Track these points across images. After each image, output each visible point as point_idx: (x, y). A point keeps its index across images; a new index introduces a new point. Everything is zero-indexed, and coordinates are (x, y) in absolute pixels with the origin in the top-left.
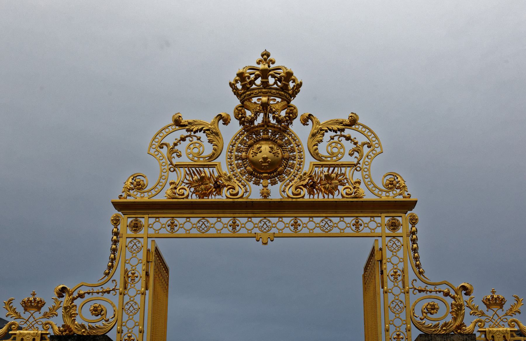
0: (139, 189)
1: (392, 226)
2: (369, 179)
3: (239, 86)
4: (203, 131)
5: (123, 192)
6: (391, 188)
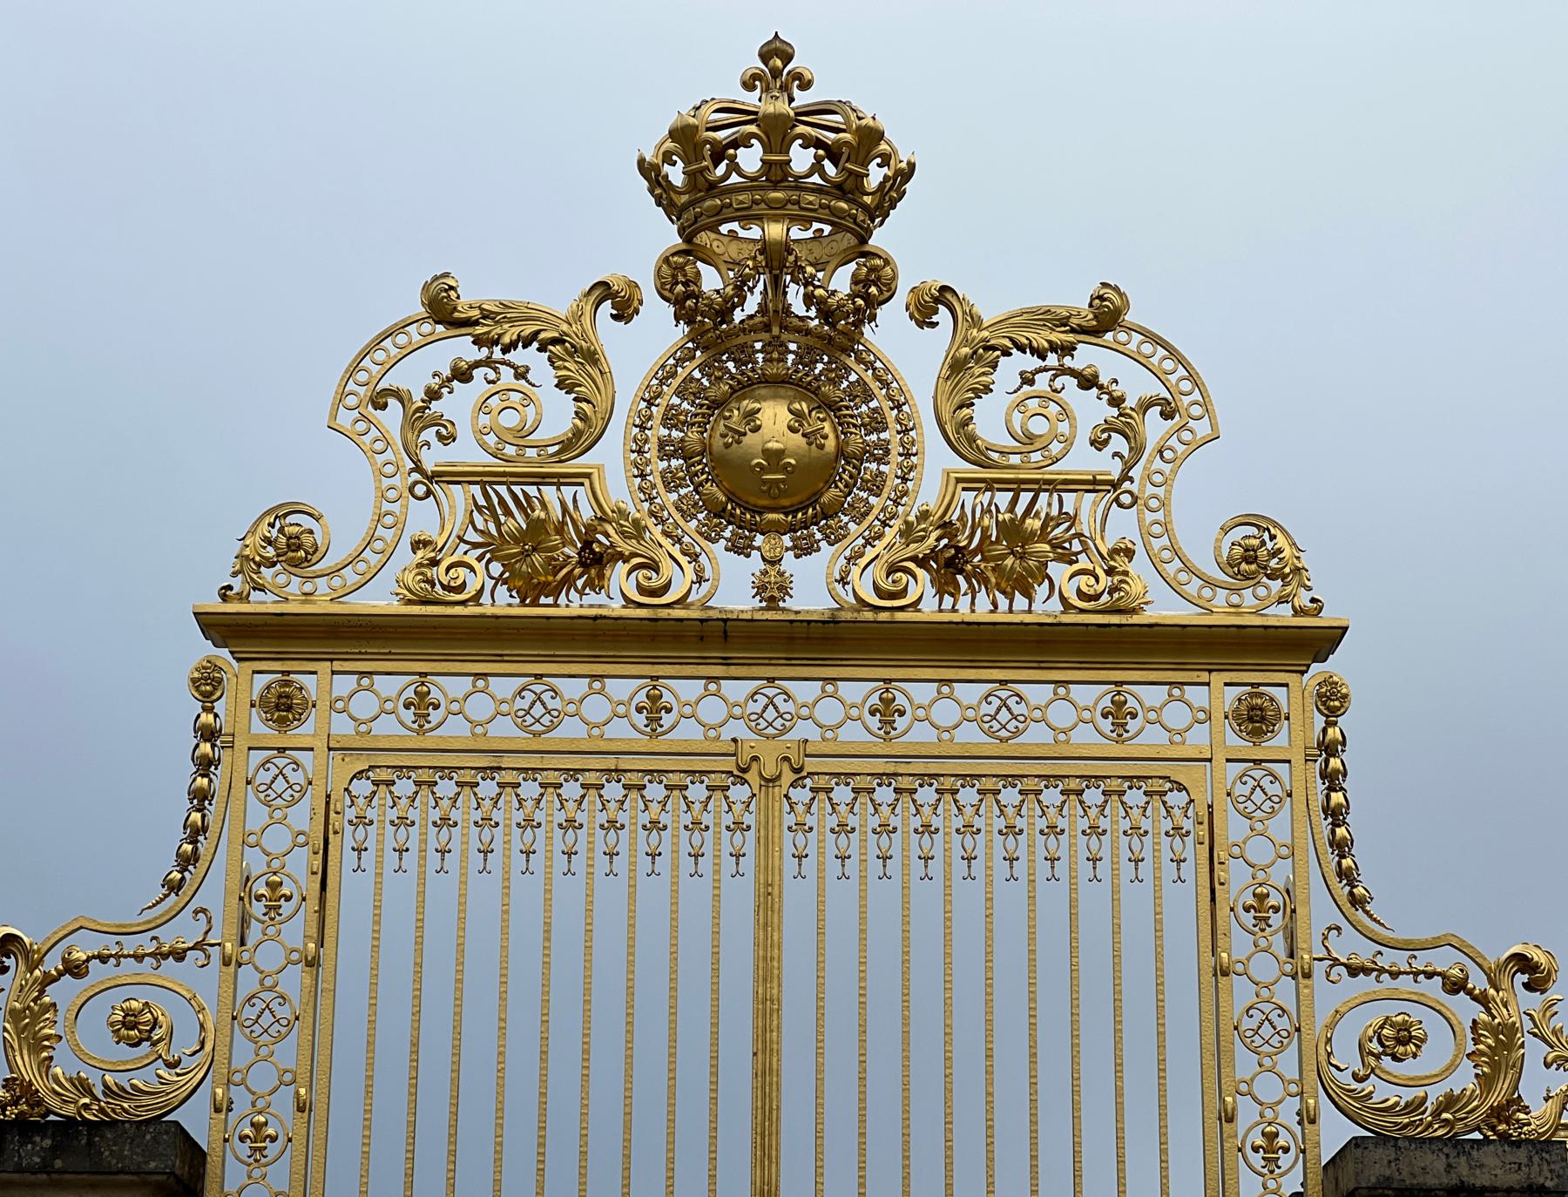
0: (296, 564)
1: (1251, 719)
2: (1165, 541)
3: (676, 174)
4: (535, 345)
5: (235, 574)
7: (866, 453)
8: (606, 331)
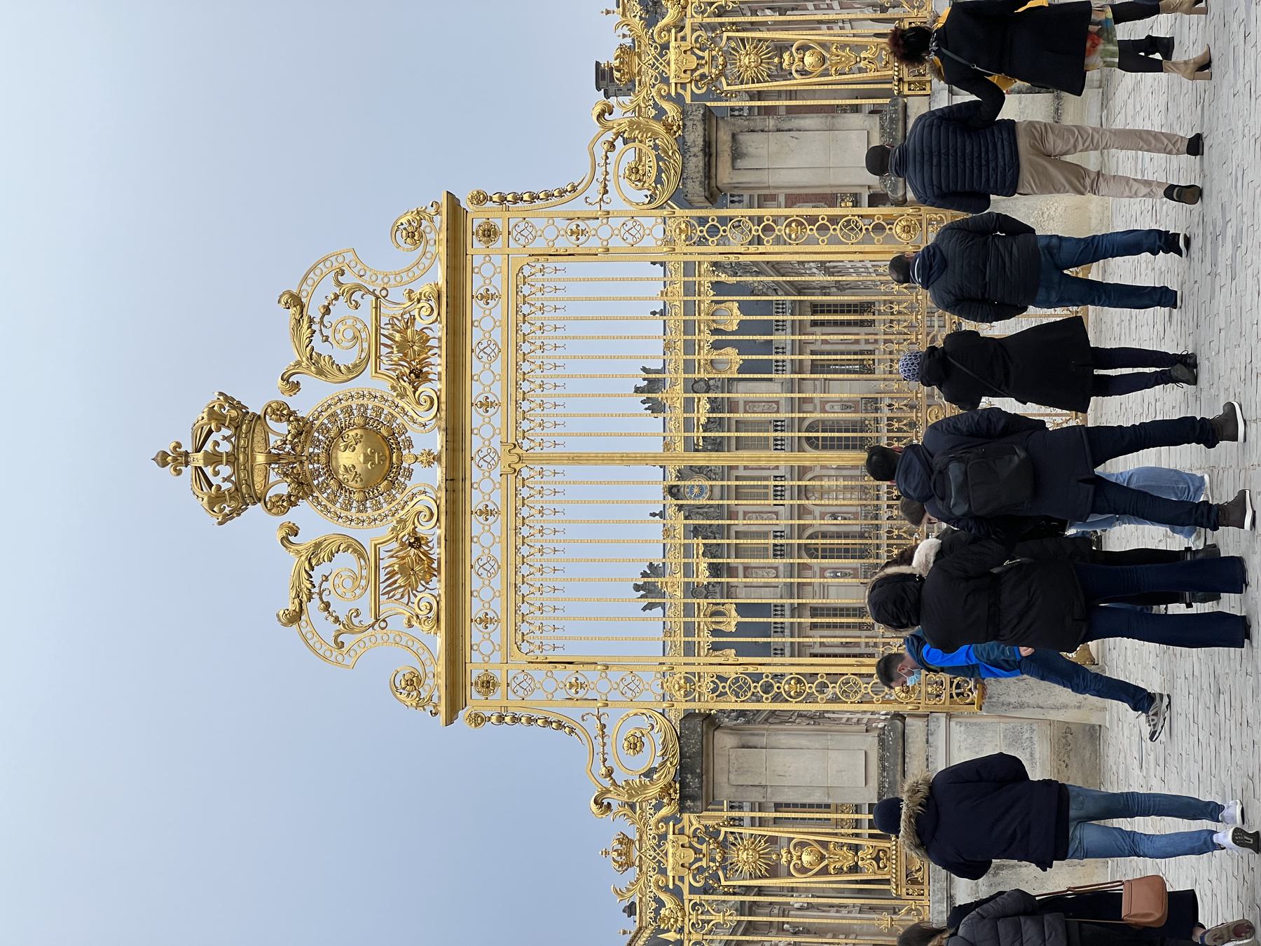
2: (404, 275)
7: (363, 415)
8: (305, 539)
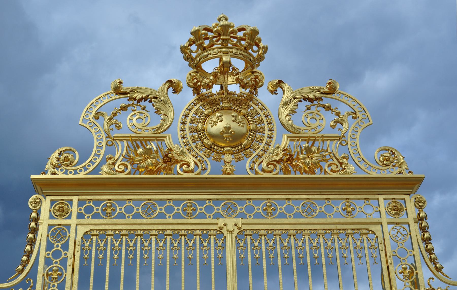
6: (386, 165)
